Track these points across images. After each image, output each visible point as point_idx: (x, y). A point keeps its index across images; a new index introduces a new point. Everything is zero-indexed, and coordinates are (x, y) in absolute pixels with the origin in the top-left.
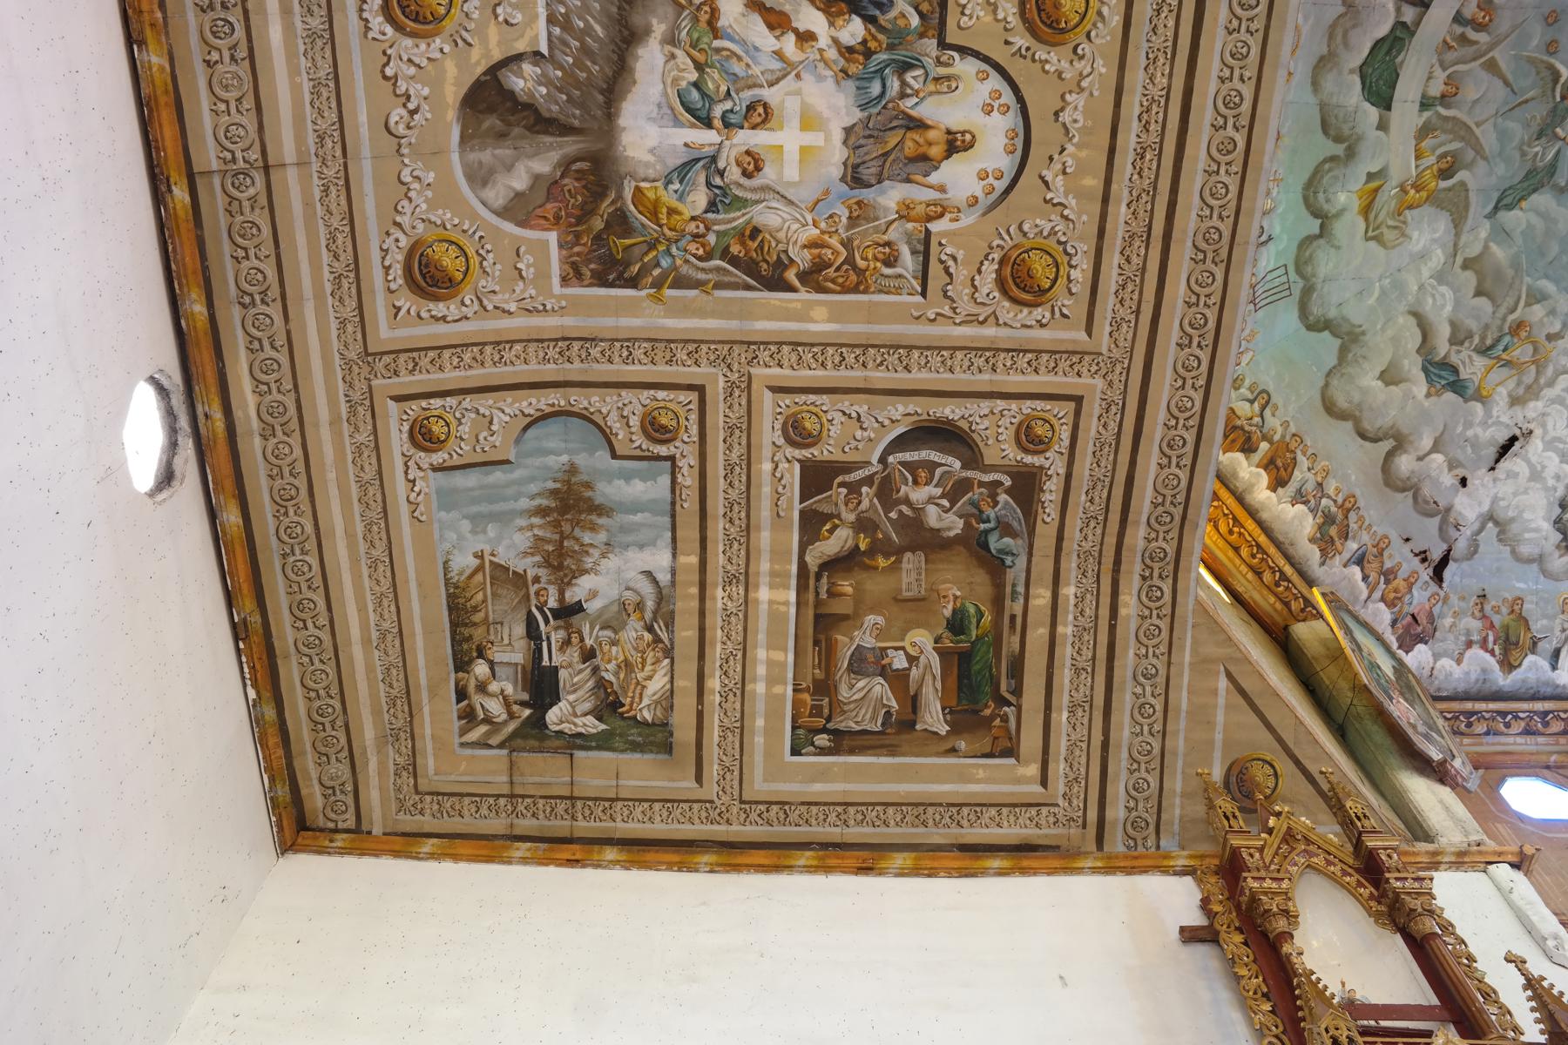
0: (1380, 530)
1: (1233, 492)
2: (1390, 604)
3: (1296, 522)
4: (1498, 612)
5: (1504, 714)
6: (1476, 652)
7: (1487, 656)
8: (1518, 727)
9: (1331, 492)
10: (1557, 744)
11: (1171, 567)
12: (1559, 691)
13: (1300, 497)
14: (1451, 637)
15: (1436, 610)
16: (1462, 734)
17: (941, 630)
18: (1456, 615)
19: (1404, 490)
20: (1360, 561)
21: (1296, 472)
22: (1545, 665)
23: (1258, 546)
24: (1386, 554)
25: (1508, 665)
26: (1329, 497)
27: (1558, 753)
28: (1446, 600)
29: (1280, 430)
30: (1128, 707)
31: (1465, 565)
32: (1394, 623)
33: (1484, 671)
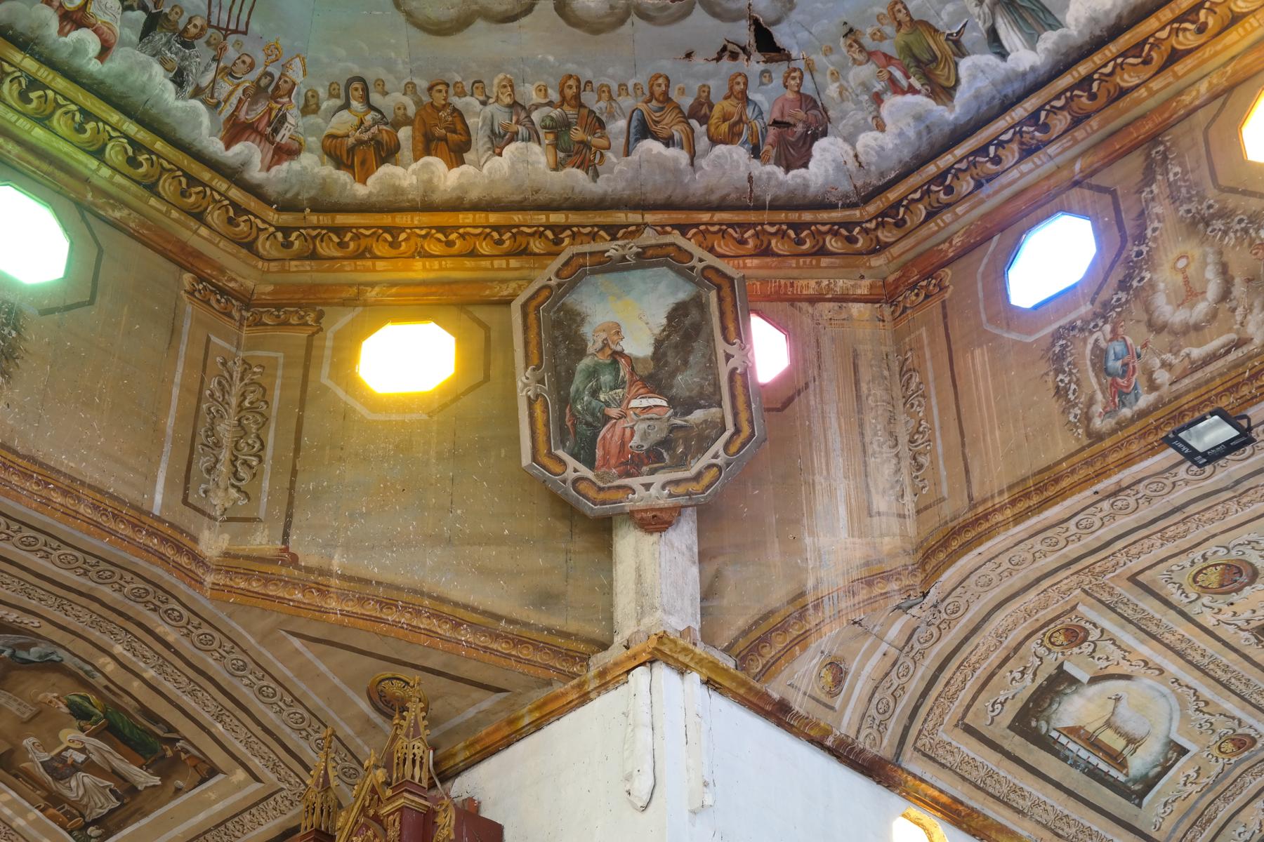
0: (642, 79)
1: (413, 208)
2: (731, 137)
3: (520, 166)
4: (883, 38)
5: (983, 150)
6: (893, 102)
7: (909, 98)
8: (1011, 154)
9: (536, 98)
10: (1076, 142)
11: (160, 593)
12: (1030, 78)
13: (499, 140)
14: (850, 105)
15: (808, 88)
16: (948, 205)
17: (76, 723)
18: (835, 76)
19: (622, 22)
20: (644, 130)
21: (470, 121)
22: (991, 59)
23: (495, 228)
24: (674, 94)
25: (943, 92)
26: (537, 106)
27: (1082, 154)
28: (811, 68)
29: (408, 101)
30: (252, 696)
31: (795, 16)
32: (756, 152)
33: (918, 118)
